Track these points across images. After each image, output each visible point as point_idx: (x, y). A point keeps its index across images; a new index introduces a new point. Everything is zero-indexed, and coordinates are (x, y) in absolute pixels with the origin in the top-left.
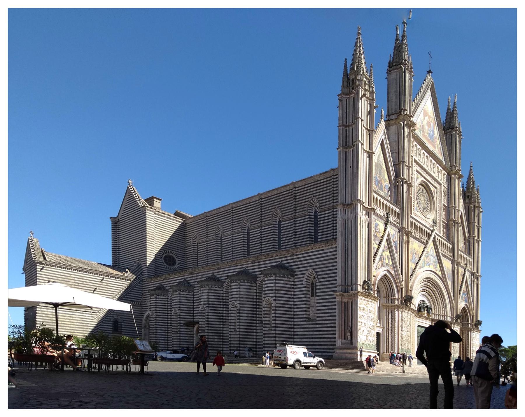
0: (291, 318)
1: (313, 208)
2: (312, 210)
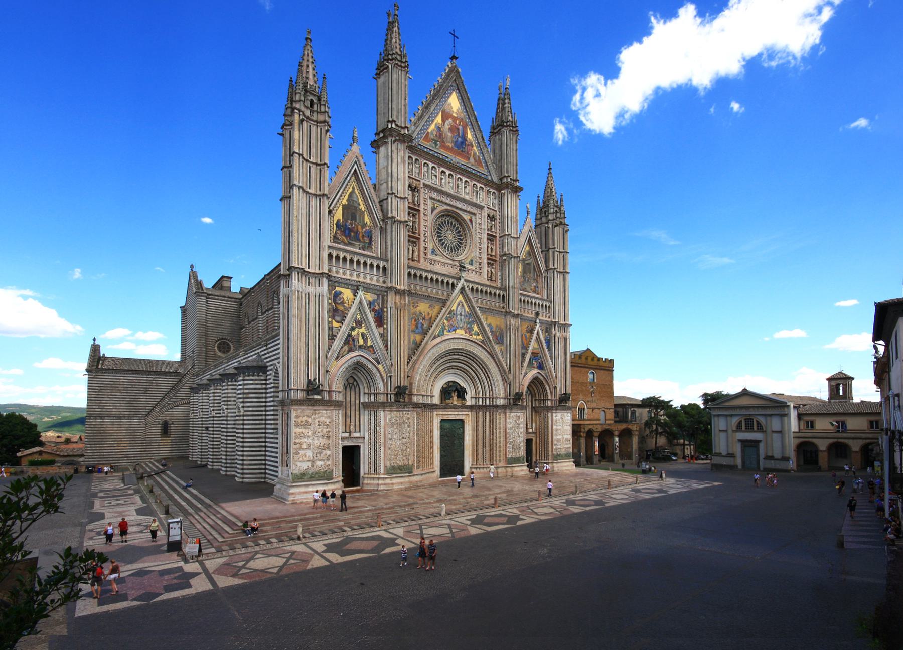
0: (262, 429)
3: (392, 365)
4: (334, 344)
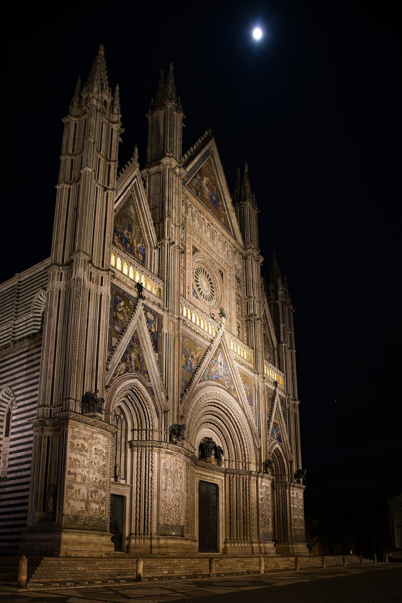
1: (41, 307)
2: (40, 309)
3: (167, 398)
4: (115, 356)
